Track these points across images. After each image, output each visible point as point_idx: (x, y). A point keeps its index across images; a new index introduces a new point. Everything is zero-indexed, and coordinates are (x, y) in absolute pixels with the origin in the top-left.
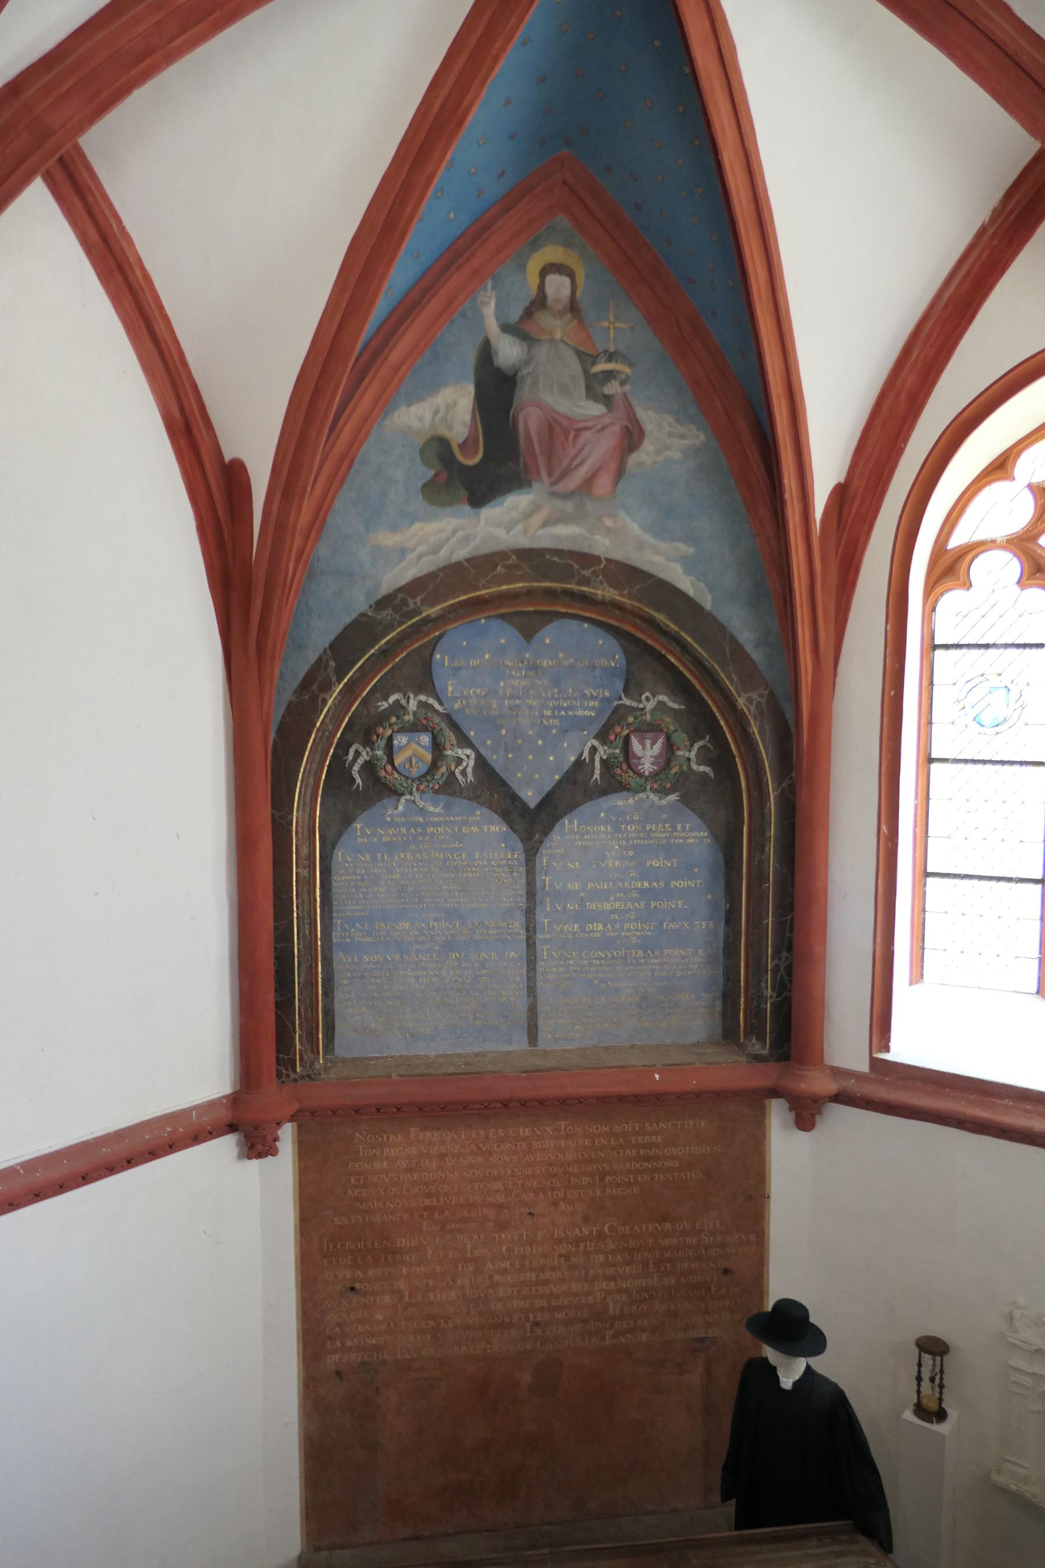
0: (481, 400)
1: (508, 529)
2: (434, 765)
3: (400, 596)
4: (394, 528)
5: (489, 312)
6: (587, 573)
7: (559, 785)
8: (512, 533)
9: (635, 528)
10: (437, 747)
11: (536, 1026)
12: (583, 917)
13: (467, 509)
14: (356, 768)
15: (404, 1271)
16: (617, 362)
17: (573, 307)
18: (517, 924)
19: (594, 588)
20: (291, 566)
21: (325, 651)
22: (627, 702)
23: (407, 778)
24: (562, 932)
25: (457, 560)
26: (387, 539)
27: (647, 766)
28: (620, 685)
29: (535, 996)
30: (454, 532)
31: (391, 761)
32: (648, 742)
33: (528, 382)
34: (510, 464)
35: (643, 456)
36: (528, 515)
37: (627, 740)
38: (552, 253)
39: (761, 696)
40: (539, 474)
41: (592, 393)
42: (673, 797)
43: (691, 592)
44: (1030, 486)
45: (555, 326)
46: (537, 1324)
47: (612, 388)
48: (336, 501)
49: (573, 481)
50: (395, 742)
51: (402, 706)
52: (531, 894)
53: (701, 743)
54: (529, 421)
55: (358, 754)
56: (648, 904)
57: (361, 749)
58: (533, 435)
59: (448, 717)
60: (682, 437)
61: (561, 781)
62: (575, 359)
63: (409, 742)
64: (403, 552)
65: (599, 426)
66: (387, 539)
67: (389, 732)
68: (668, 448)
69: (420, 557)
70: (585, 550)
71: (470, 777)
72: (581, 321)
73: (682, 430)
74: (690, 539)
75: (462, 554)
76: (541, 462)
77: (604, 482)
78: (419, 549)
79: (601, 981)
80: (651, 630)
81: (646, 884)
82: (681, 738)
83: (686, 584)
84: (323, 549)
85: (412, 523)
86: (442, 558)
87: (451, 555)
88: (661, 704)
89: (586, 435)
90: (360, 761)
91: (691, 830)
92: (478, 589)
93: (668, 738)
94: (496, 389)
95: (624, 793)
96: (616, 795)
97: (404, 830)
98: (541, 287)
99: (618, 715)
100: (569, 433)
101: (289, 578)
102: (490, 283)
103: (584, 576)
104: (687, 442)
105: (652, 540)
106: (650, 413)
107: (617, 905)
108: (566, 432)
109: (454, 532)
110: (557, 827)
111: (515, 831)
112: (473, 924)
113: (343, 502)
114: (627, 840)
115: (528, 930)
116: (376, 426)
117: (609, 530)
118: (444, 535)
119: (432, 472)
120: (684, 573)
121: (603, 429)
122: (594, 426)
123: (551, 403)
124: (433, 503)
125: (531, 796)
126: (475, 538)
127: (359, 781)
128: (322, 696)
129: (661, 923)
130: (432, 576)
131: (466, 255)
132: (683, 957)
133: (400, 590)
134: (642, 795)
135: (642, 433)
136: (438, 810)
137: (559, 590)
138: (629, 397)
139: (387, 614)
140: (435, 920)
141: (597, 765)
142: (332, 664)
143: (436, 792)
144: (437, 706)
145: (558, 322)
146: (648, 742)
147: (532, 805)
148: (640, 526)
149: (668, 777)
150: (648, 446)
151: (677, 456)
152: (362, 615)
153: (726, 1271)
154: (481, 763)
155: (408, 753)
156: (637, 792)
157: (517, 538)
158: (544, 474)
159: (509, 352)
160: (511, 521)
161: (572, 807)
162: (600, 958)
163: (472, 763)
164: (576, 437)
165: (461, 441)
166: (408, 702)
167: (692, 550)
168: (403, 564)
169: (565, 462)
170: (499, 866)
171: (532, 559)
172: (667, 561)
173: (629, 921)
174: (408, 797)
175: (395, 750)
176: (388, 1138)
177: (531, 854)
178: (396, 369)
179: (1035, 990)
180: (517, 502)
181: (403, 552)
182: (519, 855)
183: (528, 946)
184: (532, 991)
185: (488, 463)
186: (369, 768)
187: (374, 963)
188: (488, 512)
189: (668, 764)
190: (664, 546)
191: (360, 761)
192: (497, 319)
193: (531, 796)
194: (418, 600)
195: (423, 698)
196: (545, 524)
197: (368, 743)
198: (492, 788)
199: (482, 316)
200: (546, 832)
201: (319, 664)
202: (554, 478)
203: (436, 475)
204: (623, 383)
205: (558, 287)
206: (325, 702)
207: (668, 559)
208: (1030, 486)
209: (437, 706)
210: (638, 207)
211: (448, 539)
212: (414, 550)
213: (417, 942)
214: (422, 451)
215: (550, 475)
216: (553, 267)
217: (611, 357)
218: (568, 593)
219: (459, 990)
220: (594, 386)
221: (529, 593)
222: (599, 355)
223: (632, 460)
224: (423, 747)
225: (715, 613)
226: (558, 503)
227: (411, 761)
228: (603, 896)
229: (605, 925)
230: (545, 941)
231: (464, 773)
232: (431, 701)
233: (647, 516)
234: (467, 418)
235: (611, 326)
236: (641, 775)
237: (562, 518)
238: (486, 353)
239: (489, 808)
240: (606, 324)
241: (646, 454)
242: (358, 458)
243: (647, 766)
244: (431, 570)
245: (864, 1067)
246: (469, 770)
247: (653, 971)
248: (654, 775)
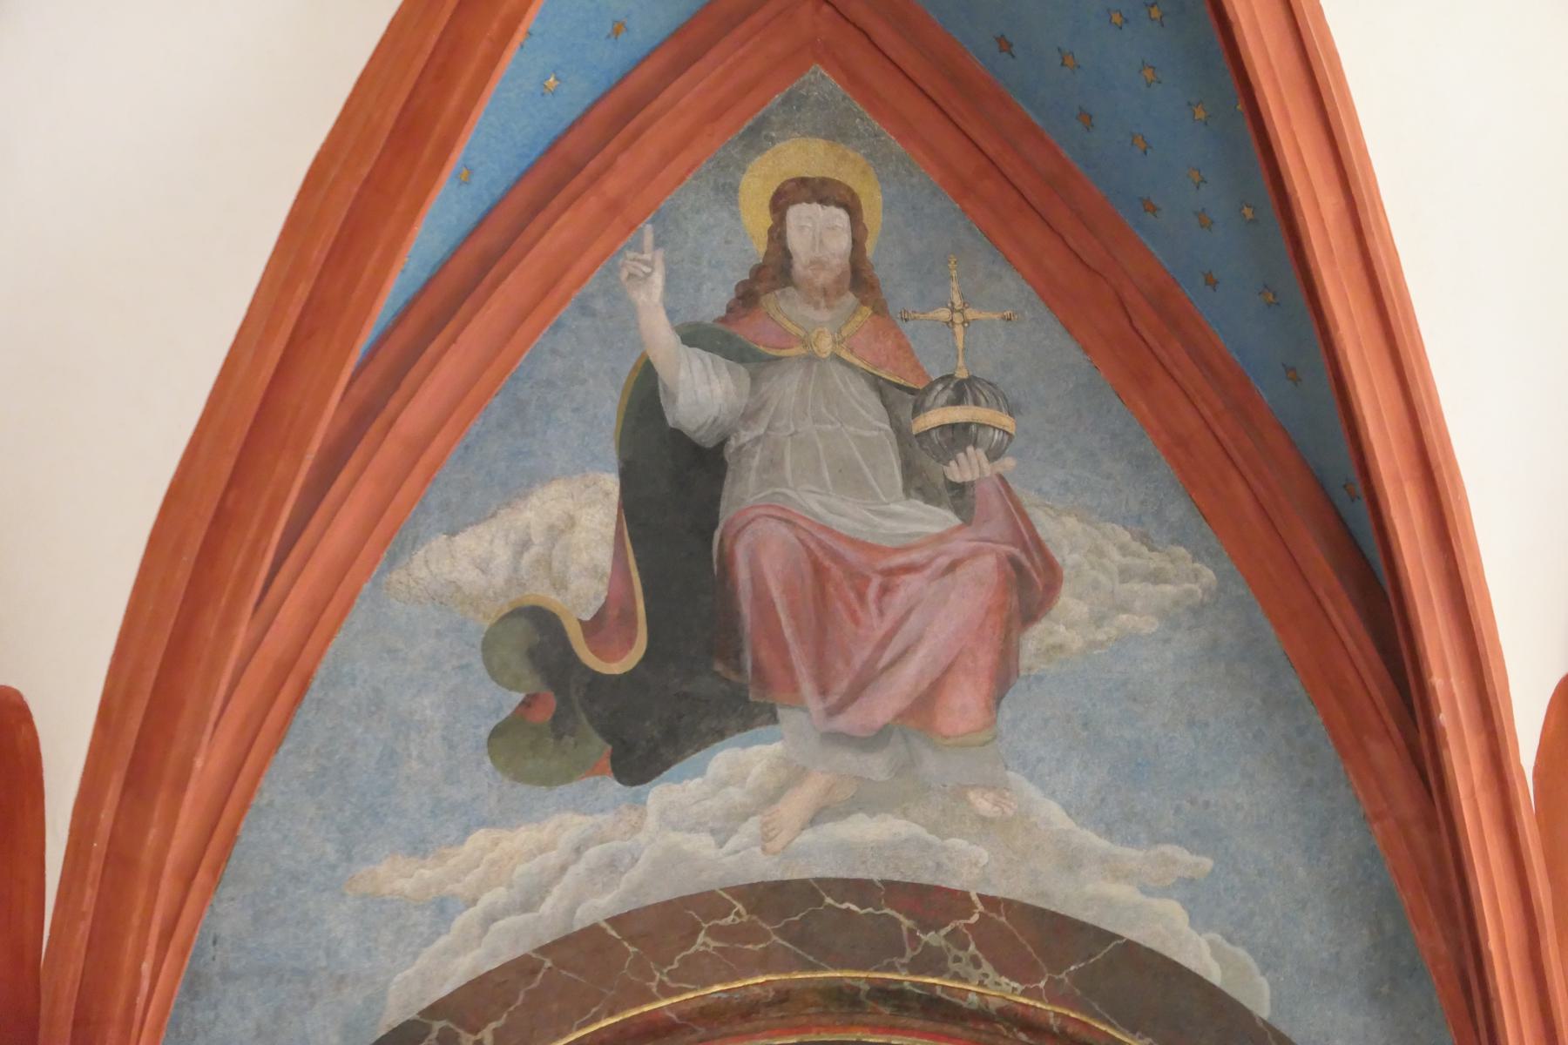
0: (636, 511)
1: (721, 835)
3: (438, 1025)
4: (419, 848)
5: (650, 299)
6: (932, 938)
8: (732, 843)
9: (1053, 814)
13: (611, 787)
16: (976, 403)
17: (860, 277)
19: (956, 976)
20: (146, 967)
25: (588, 923)
26: (401, 877)
30: (578, 851)
33: (755, 462)
34: (719, 667)
35: (1062, 629)
36: (771, 797)
38: (800, 155)
40: (795, 688)
41: (917, 483)
43: (1215, 974)
45: (814, 323)
47: (968, 467)
48: (264, 783)
49: (885, 703)
54: (761, 556)
58: (776, 592)
60: (1156, 577)
62: (873, 400)
64: (443, 909)
65: (944, 561)
66: (401, 877)
68: (1124, 608)
69: (490, 918)
70: (926, 879)
72: (880, 310)
73: (1155, 561)
74: (1200, 836)
75: (599, 906)
76: (799, 657)
77: (964, 702)
78: (486, 899)
83: (1199, 953)
84: (227, 914)
85: (467, 831)
86: (552, 917)
87: (571, 911)
89: (911, 585)
92: (653, 999)
94: (675, 485)
98: (777, 234)
100: (868, 580)
101: (140, 1001)
102: (648, 232)
103: (927, 944)
104: (1169, 589)
105: (1103, 844)
106: (1071, 522)
108: (860, 582)
109: (578, 851)
113: (283, 785)
116: (366, 586)
117: (984, 820)
118: (553, 859)
119: (518, 697)
120: (1192, 924)
121: (952, 567)
122: (931, 560)
123: (817, 508)
124: (519, 777)
126: (635, 860)
130: (523, 967)
131: (593, 165)
133: (434, 1010)
135: (1052, 574)
137: (866, 987)
138: (1015, 487)
145: (824, 315)
148: (1066, 807)
150: (1070, 604)
151: (1147, 625)
157: (747, 858)
158: (807, 688)
159: (701, 392)
160: (728, 815)
164: (885, 590)
165: (587, 617)
167: (1207, 863)
168: (441, 942)
169: (861, 656)
178: (418, 447)
180: (735, 766)
181: (443, 909)
185: (665, 664)
188: (661, 794)
190: (1133, 856)
192: (671, 313)
196: (816, 818)
199: (633, 310)
202: (833, 699)
203: (526, 704)
204: (994, 454)
205: (818, 233)
207: (1145, 890)
210: (1004, 45)
211: (563, 869)
212: (474, 902)
214: (489, 645)
215: (823, 692)
216: (809, 182)
217: (961, 392)
218: (887, 994)
220: (923, 465)
221: (784, 997)
222: (931, 386)
223: (1033, 641)
225: (1283, 1028)
226: (849, 760)
234: (603, 556)
235: (958, 318)
237: (864, 801)
238: (646, 397)
240: (944, 314)
241: (1066, 625)
242: (321, 671)
244: (519, 952)
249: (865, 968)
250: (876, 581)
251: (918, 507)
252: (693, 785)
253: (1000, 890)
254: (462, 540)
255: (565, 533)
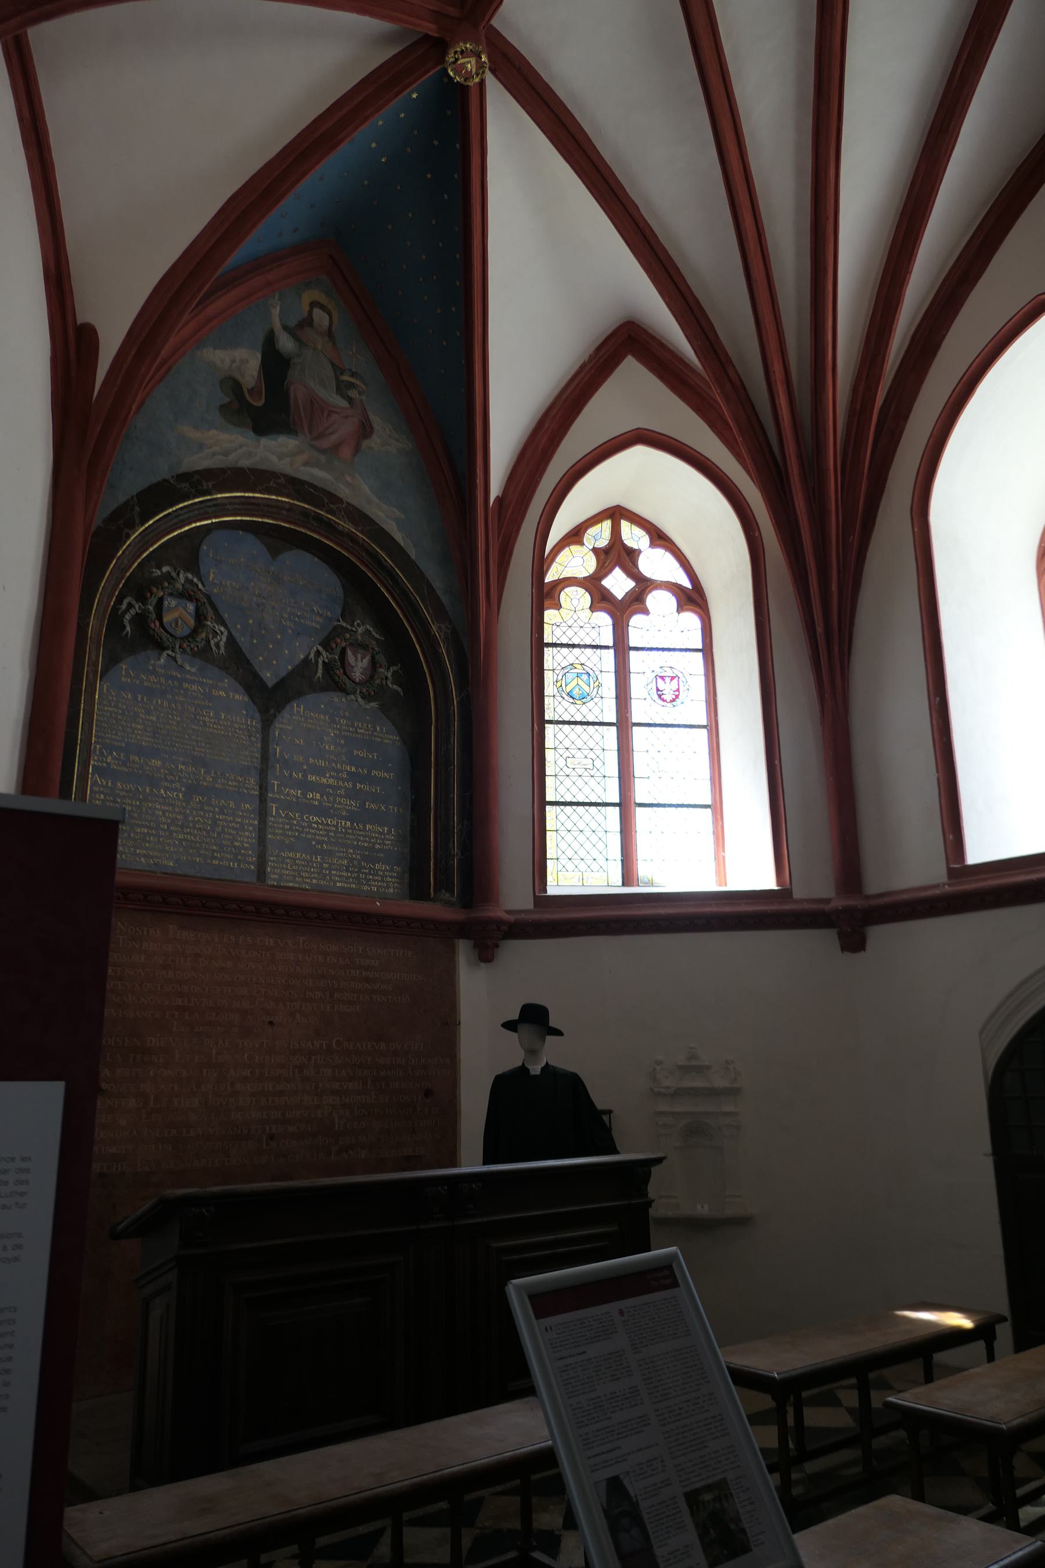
2: (194, 632)
3: (197, 477)
5: (276, 312)
7: (290, 674)
10: (200, 617)
11: (265, 873)
12: (305, 786)
14: (128, 617)
15: (151, 1073)
17: (330, 333)
18: (252, 781)
21: (132, 497)
22: (344, 625)
23: (171, 635)
24: (288, 794)
26: (192, 434)
27: (358, 675)
28: (339, 611)
29: (265, 846)
30: (241, 446)
31: (160, 618)
32: (359, 656)
37: (343, 652)
39: (447, 628)
42: (374, 704)
43: (402, 544)
44: (595, 550)
46: (271, 1138)
47: (353, 393)
49: (327, 443)
50: (166, 603)
51: (172, 578)
52: (265, 757)
53: (395, 668)
54: (297, 392)
55: (130, 606)
56: (355, 786)
57: (134, 602)
59: (208, 597)
60: (397, 440)
61: (293, 671)
63: (176, 606)
64: (201, 447)
66: (192, 434)
67: (161, 594)
69: (214, 454)
71: (222, 648)
75: (245, 463)
77: (346, 452)
79: (318, 842)
80: (364, 572)
81: (353, 769)
82: (381, 659)
83: (398, 537)
88: (368, 632)
90: (133, 612)
91: (387, 733)
93: (373, 658)
94: (275, 365)
95: (339, 694)
96: (333, 694)
97: (163, 680)
98: (310, 313)
99: (336, 632)
107: (331, 781)
109: (241, 446)
110: (288, 707)
111: (254, 703)
112: (216, 773)
114: (340, 730)
115: (261, 788)
121: (346, 417)
125: (269, 677)
127: (128, 629)
128: (127, 530)
129: (364, 802)
130: (222, 471)
132: (381, 833)
134: (352, 697)
136: (193, 670)
139: (185, 486)
140: (183, 763)
141: (320, 666)
142: (137, 509)
143: (194, 655)
144: (200, 586)
146: (359, 656)
147: (270, 685)
149: (371, 689)
150: (375, 437)
152: (165, 480)
153: (428, 1093)
154: (231, 641)
155: (176, 615)
156: (348, 694)
157: (284, 466)
158: (306, 430)
159: (286, 343)
161: (299, 694)
162: (317, 823)
163: (224, 639)
164: (328, 415)
166: (178, 574)
170: (240, 729)
171: (295, 486)
172: (386, 516)
173: (340, 796)
174: (170, 652)
175: (164, 610)
176: (148, 932)
177: (267, 724)
179: (620, 884)
180: (286, 443)
181: (201, 447)
182: (256, 723)
183: (261, 801)
184: (262, 840)
186: (141, 620)
187: (127, 791)
188: (264, 441)
189: (372, 677)
191: (133, 612)
193: (269, 677)
194: (210, 485)
195: (190, 576)
197: (142, 599)
198: (237, 663)
200: (280, 708)
201: (126, 506)
204: (360, 393)
206: (128, 536)
208: (595, 550)
209: (200, 586)
211: (236, 449)
213: (167, 780)
215: (310, 433)
217: (353, 374)
218: (319, 518)
219: (200, 829)
220: (342, 388)
221: (291, 508)
223: (365, 443)
224: (189, 614)
227: (177, 622)
228: (320, 772)
229: (322, 796)
230: (274, 800)
231: (217, 645)
232: (195, 580)
233: (375, 484)
234: (255, 374)
236: (354, 682)
239: (235, 679)
241: (374, 442)
243: (358, 675)
245: (530, 905)
246: (222, 644)
247: (358, 841)
248: (361, 683)
249: (315, 507)
250: (325, 414)
251: (339, 398)
252: (274, 442)
253: (350, 501)
254: (217, 351)
255: (247, 363)
